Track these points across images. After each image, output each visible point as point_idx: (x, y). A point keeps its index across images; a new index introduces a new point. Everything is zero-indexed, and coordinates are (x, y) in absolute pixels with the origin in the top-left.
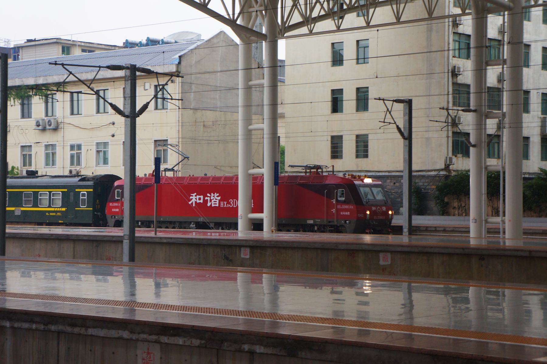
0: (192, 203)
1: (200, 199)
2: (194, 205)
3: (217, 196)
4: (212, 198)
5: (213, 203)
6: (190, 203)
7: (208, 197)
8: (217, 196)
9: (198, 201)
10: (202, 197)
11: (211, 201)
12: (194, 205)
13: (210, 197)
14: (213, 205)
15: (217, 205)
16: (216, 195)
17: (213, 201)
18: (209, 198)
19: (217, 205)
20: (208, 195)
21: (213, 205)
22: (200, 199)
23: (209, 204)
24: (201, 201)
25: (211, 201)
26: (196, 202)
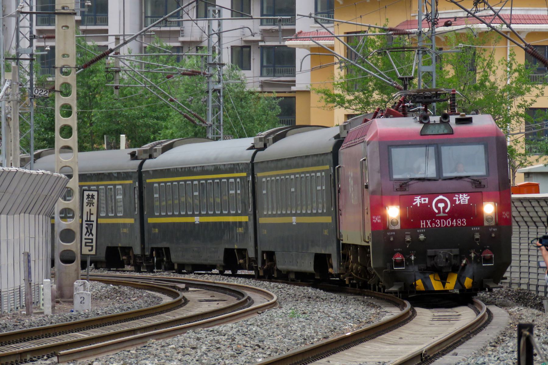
2: (419, 205)
4: (460, 198)
5: (462, 202)
11: (459, 200)
12: (419, 205)
13: (459, 197)
14: (462, 203)
15: (467, 203)
17: (461, 200)
18: (457, 199)
19: (467, 203)
20: (456, 196)
21: (462, 203)
23: (457, 202)
25: (459, 200)
26: (420, 203)
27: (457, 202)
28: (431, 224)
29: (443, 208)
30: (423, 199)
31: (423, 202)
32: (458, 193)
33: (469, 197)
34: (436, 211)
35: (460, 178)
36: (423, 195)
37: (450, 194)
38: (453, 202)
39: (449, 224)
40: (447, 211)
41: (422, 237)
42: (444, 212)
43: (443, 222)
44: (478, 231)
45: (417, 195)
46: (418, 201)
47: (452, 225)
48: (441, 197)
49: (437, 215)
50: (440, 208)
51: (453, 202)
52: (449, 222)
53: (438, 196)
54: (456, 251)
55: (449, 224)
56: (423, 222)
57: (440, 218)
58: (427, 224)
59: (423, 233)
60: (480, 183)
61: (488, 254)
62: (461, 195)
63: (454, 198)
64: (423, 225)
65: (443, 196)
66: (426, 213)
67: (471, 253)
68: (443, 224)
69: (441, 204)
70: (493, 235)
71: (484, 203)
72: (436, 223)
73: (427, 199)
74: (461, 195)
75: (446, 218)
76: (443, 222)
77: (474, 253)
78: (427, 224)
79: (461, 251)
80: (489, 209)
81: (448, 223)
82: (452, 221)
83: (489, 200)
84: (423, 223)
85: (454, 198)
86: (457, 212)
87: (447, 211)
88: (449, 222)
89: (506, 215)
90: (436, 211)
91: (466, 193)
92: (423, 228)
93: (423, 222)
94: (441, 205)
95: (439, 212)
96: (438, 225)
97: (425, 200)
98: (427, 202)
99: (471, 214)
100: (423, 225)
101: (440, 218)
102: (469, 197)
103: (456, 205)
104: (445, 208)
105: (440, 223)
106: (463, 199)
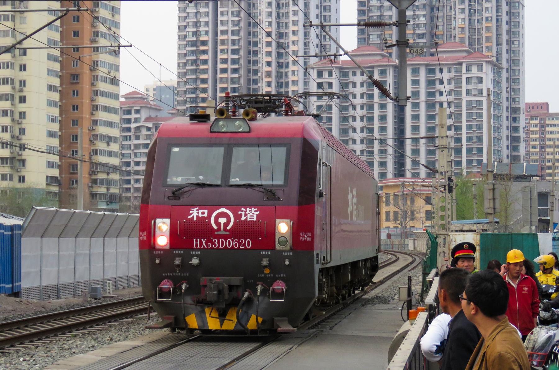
0: (193, 217)
1: (203, 213)
3: (255, 211)
5: (249, 217)
6: (189, 217)
7: (242, 211)
8: (255, 211)
9: (201, 215)
10: (206, 211)
11: (246, 215)
13: (245, 212)
14: (249, 220)
15: (255, 220)
16: (253, 209)
17: (248, 215)
18: (243, 213)
19: (255, 220)
20: (243, 209)
21: (249, 220)
22: (203, 213)
23: (243, 218)
24: (206, 215)
25: (246, 215)
27: (243, 218)
29: (224, 224)
30: (200, 211)
32: (246, 206)
33: (258, 213)
34: (215, 227)
35: (251, 186)
36: (201, 206)
37: (235, 207)
38: (237, 217)
39: (229, 246)
40: (229, 228)
41: (195, 261)
42: (225, 229)
43: (222, 242)
44: (265, 256)
45: (194, 206)
48: (223, 210)
49: (216, 233)
50: (220, 223)
51: (237, 217)
52: (229, 242)
53: (220, 209)
54: (236, 280)
55: (229, 245)
56: (197, 241)
57: (218, 236)
58: (201, 243)
59: (197, 256)
60: (274, 194)
61: (279, 286)
62: (248, 209)
63: (240, 213)
64: (197, 245)
65: (226, 208)
66: (203, 229)
67: (258, 285)
68: (222, 245)
69: (222, 218)
70: (287, 263)
71: (277, 221)
72: (213, 243)
74: (248, 209)
75: (225, 237)
76: (222, 242)
77: (262, 285)
78: (201, 243)
79: (245, 280)
80: (283, 227)
81: (232, 243)
83: (283, 217)
84: (196, 243)
85: (240, 213)
86: (241, 230)
87: (229, 228)
88: (229, 242)
89: (305, 237)
91: (255, 206)
92: (197, 249)
93: (197, 241)
94: (222, 221)
95: (219, 229)
96: (215, 245)
98: (206, 215)
99: (262, 235)
100: (197, 245)
101: (218, 236)
102: (258, 213)
103: (241, 221)
104: (226, 224)
105: (218, 243)
106: (251, 214)
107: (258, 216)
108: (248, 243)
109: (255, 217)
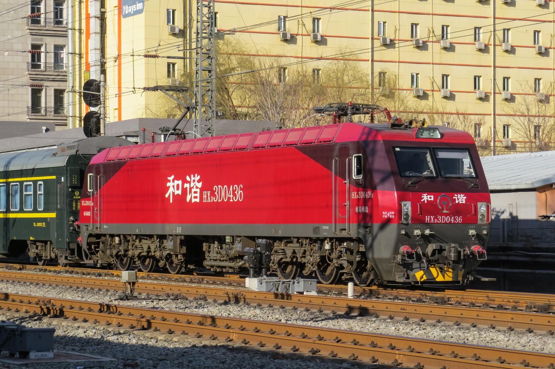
1: (431, 198)
11: (458, 199)
15: (464, 202)
19: (464, 202)
23: (457, 202)
25: (458, 199)
26: (427, 200)
27: (457, 202)
28: (434, 220)
31: (429, 200)
33: (465, 198)
45: (425, 192)
46: (426, 198)
47: (451, 222)
72: (438, 219)
73: (432, 196)
78: (431, 219)
82: (451, 218)
90: (440, 207)
92: (427, 223)
97: (431, 198)
102: (465, 198)
105: (441, 219)
106: (461, 199)
107: (466, 200)
108: (459, 220)
109: (464, 200)
